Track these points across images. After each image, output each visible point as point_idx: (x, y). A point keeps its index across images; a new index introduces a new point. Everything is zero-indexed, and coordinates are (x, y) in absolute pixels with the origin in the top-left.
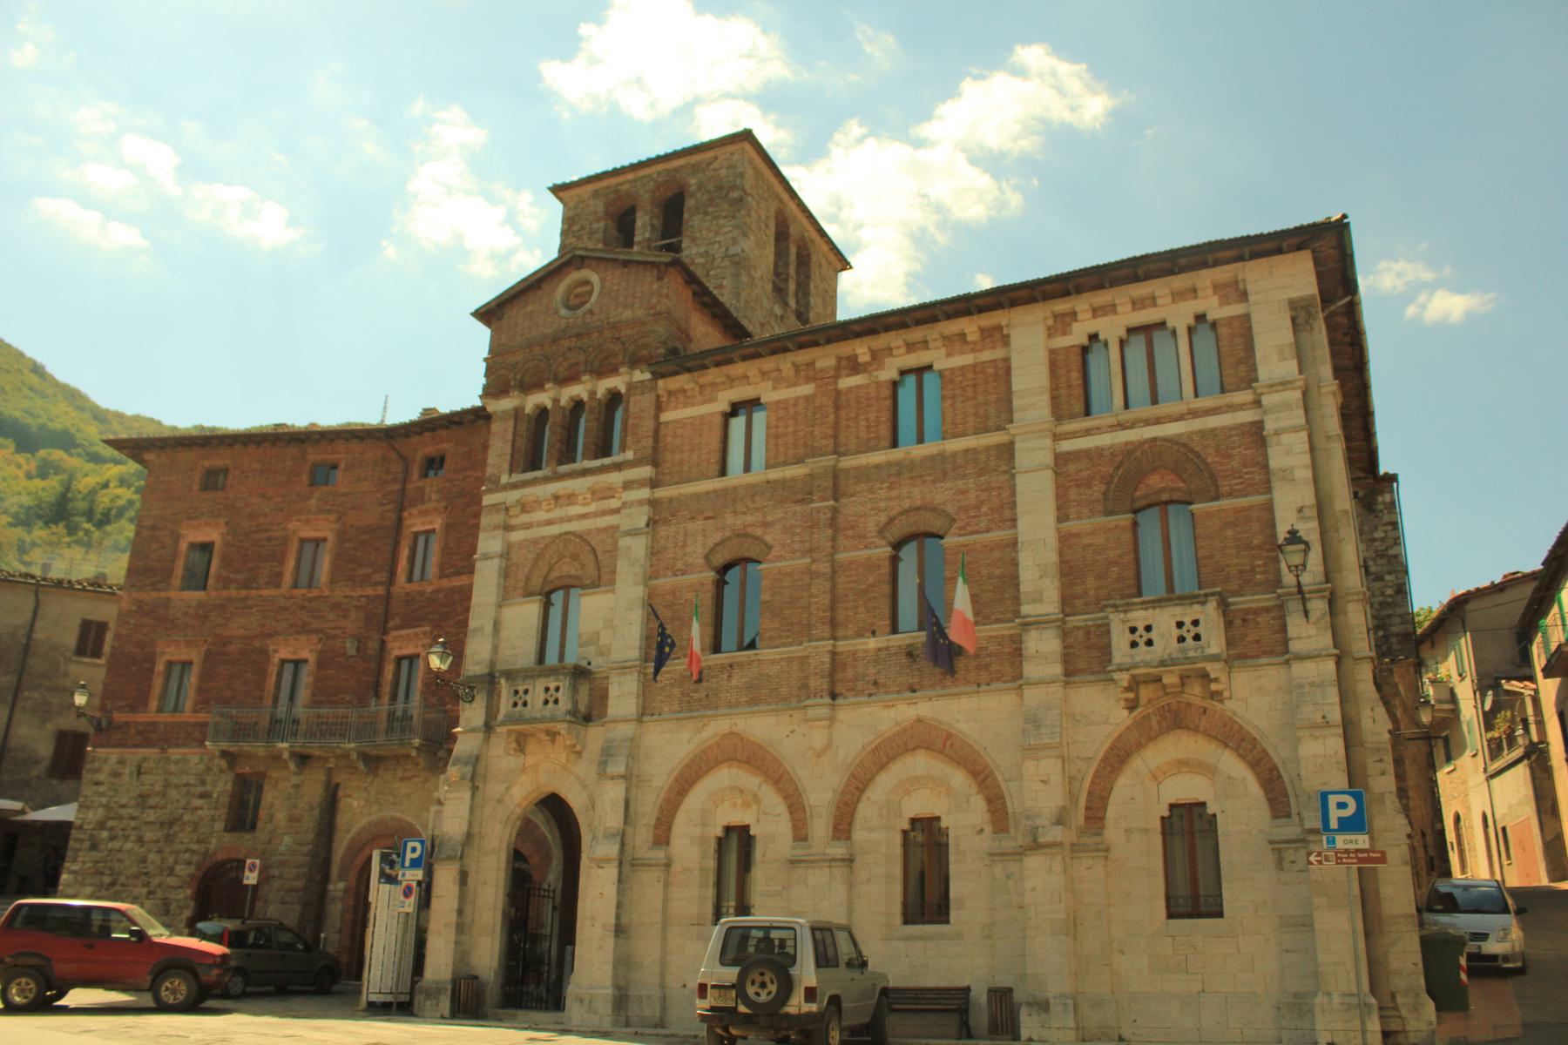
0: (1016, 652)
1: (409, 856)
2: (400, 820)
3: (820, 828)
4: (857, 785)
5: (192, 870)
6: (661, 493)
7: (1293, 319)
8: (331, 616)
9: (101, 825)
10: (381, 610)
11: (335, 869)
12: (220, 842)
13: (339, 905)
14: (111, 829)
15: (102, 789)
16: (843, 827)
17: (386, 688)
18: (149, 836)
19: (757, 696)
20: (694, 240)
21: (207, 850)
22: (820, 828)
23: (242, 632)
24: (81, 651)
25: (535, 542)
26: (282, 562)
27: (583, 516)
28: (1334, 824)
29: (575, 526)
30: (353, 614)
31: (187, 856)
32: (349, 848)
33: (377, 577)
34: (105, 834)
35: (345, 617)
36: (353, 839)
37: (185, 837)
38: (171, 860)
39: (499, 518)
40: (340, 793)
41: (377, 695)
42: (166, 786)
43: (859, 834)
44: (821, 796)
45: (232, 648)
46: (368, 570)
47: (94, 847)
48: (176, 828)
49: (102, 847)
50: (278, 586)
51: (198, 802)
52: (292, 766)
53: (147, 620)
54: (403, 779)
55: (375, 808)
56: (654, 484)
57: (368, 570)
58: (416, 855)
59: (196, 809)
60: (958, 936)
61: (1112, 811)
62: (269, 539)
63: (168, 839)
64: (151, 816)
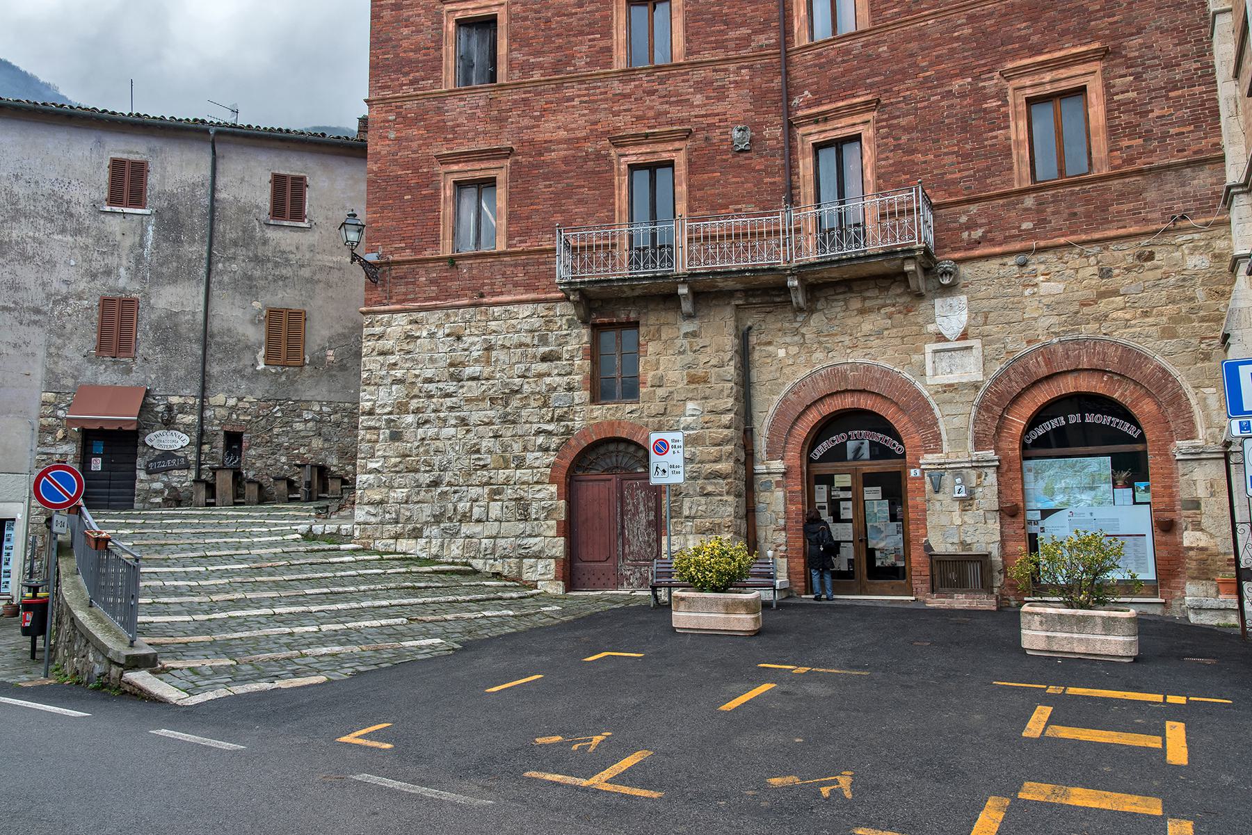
2: (868, 368)
5: (551, 458)
8: (698, 99)
9: (402, 408)
10: (777, 82)
11: (761, 444)
12: (591, 418)
13: (779, 494)
14: (417, 411)
15: (392, 359)
17: (807, 190)
18: (475, 417)
21: (569, 431)
23: (562, 134)
24: (278, 211)
26: (607, 33)
30: (733, 94)
31: (540, 440)
32: (780, 413)
33: (762, 39)
34: (410, 419)
35: (722, 97)
36: (785, 400)
38: (517, 447)
40: (753, 340)
41: (792, 200)
42: (489, 349)
45: (548, 157)
46: (745, 31)
47: (396, 436)
48: (515, 402)
49: (408, 435)
50: (609, 64)
51: (543, 367)
52: (687, 306)
54: (862, 312)
55: (819, 355)
57: (745, 31)
59: (540, 376)
63: (505, 419)
64: (474, 389)
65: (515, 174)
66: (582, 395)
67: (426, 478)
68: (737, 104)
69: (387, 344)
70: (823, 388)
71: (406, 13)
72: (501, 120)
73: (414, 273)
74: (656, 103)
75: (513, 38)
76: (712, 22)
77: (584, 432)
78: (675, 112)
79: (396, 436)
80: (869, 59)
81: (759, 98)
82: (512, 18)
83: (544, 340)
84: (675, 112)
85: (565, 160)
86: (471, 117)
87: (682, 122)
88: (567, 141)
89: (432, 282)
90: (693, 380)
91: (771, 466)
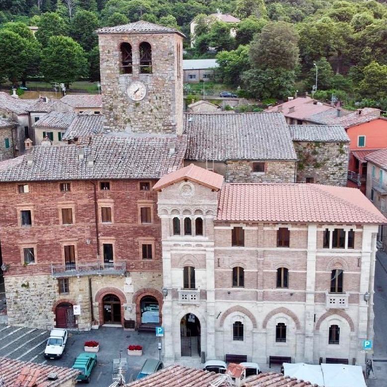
0: (305, 295)
1: (158, 331)
3: (260, 326)
4: (268, 317)
5: (52, 306)
6: (217, 248)
7: (372, 236)
8: (79, 233)
9: (16, 297)
10: (95, 230)
11: (94, 299)
13: (98, 308)
16: (264, 326)
19: (244, 298)
20: (157, 70)
22: (260, 326)
23: (49, 239)
25: (181, 254)
26: (58, 217)
27: (193, 250)
28: (365, 346)
29: (191, 252)
31: (49, 303)
33: (92, 220)
34: (19, 300)
35: (84, 233)
36: (98, 292)
37: (46, 299)
39: (169, 248)
43: (268, 327)
44: (260, 321)
46: (88, 218)
51: (49, 288)
53: (12, 237)
55: (104, 285)
56: (215, 246)
57: (88, 218)
58: (161, 331)
60: (288, 346)
61: (321, 327)
62: (51, 209)
64: (33, 293)
65: (38, 247)
66: (57, 294)
67: (24, 312)
68: (87, 234)
69: (11, 284)
70: (105, 290)
71: (6, 208)
72: (34, 235)
73: (16, 269)
74: (69, 232)
75: (35, 216)
76: (81, 216)
77: (58, 301)
78: (74, 235)
79: (16, 303)
80: (114, 230)
81: (92, 233)
82: (35, 211)
83: (48, 283)
84: (74, 235)
85: (50, 245)
86: (26, 234)
87: (75, 237)
88: (50, 240)
89: (21, 270)
90: (80, 290)
91: (96, 304)
